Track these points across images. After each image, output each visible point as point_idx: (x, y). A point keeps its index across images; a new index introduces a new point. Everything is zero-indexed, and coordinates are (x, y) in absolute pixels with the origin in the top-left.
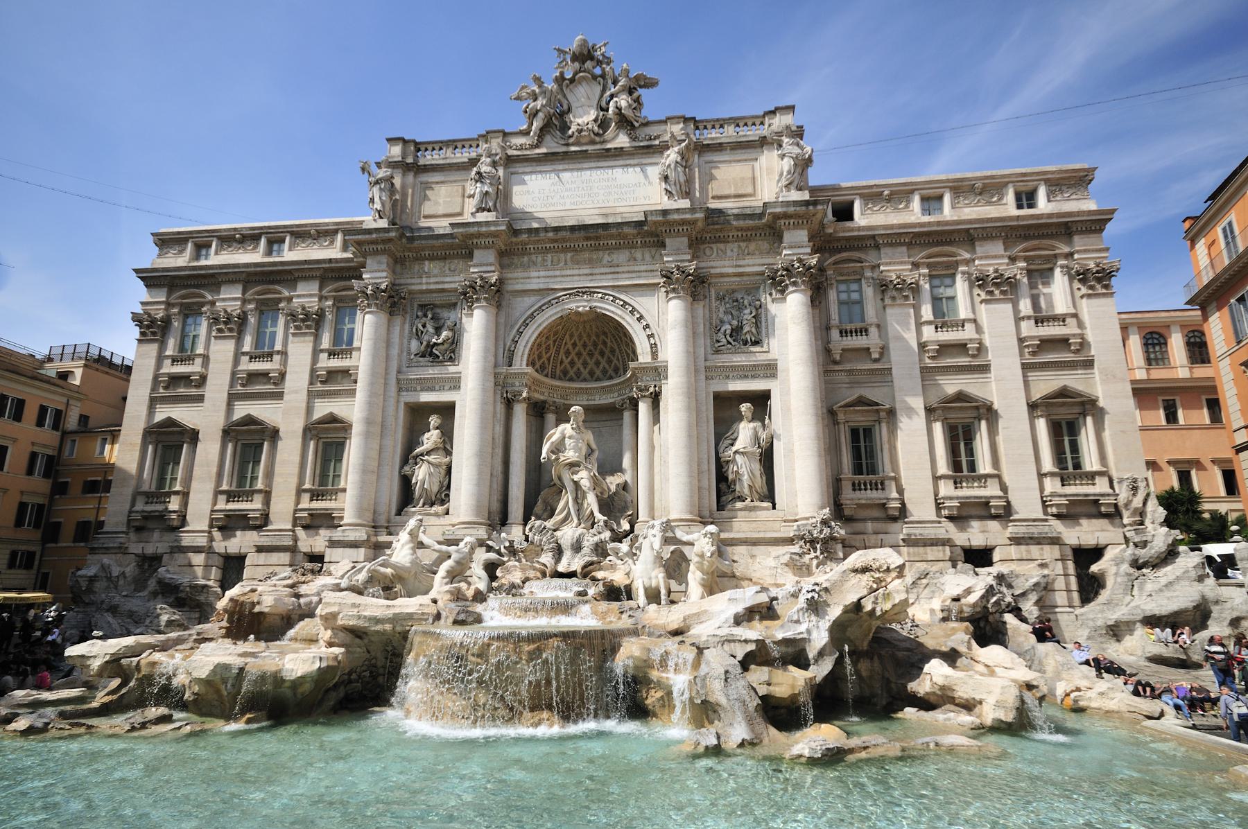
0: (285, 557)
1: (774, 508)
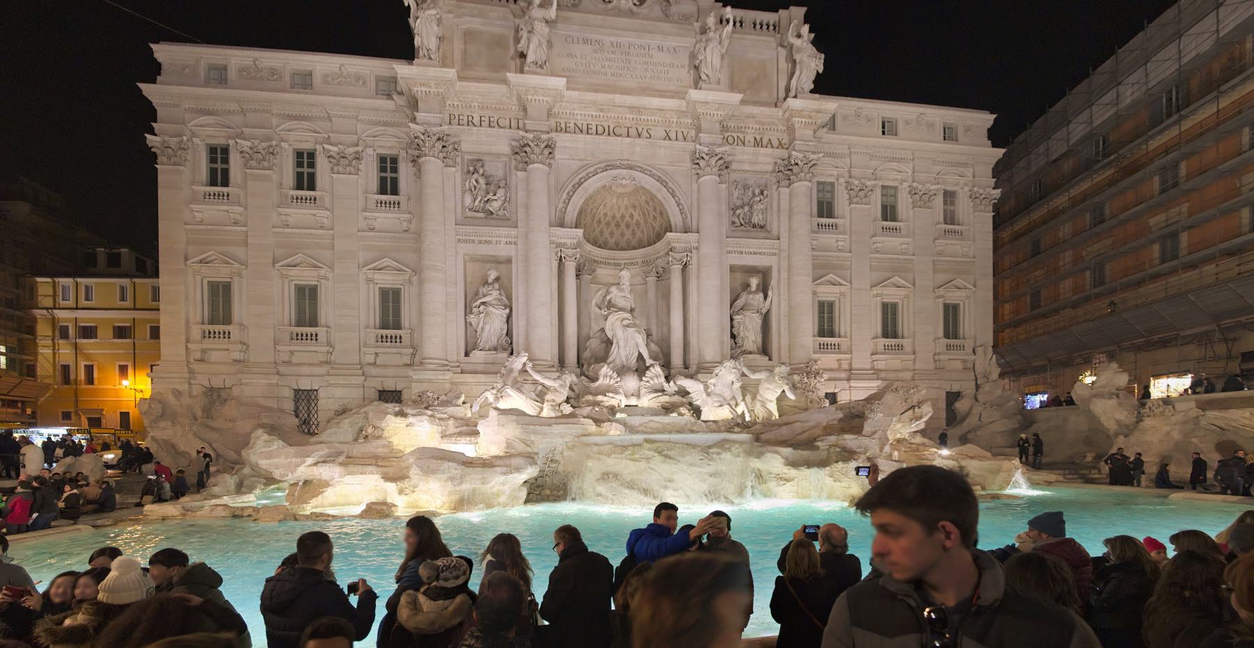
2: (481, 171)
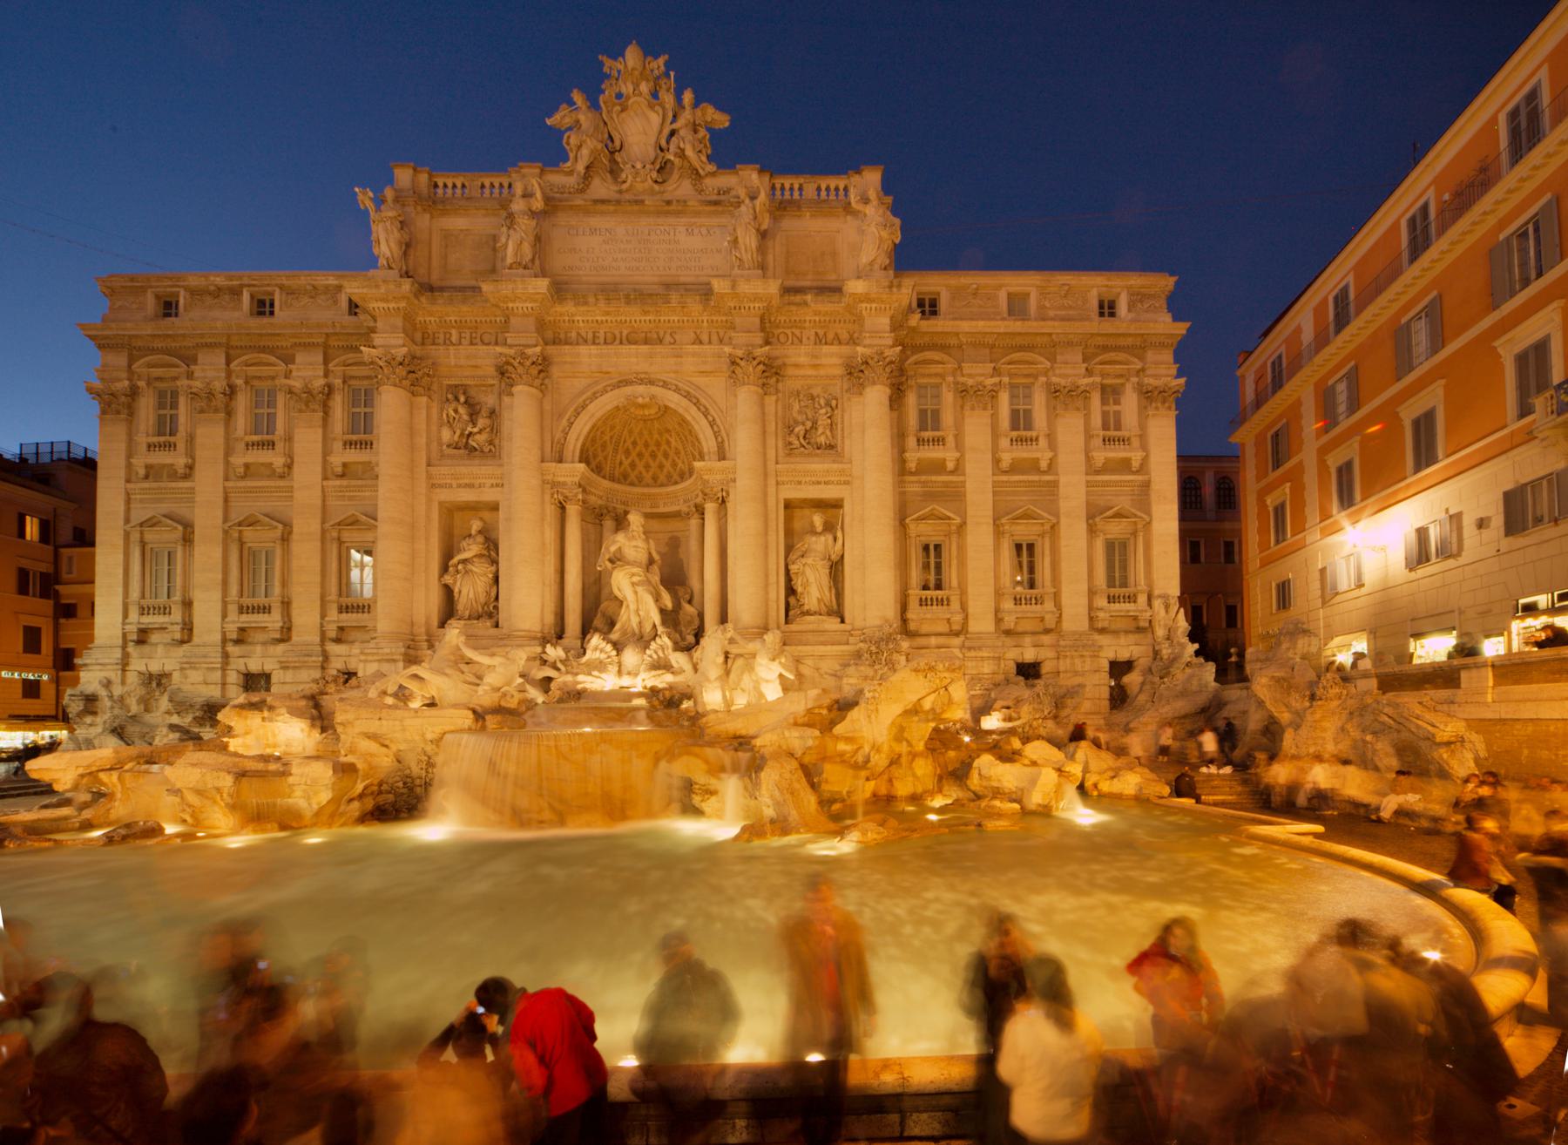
1: (843, 621)
2: (462, 399)
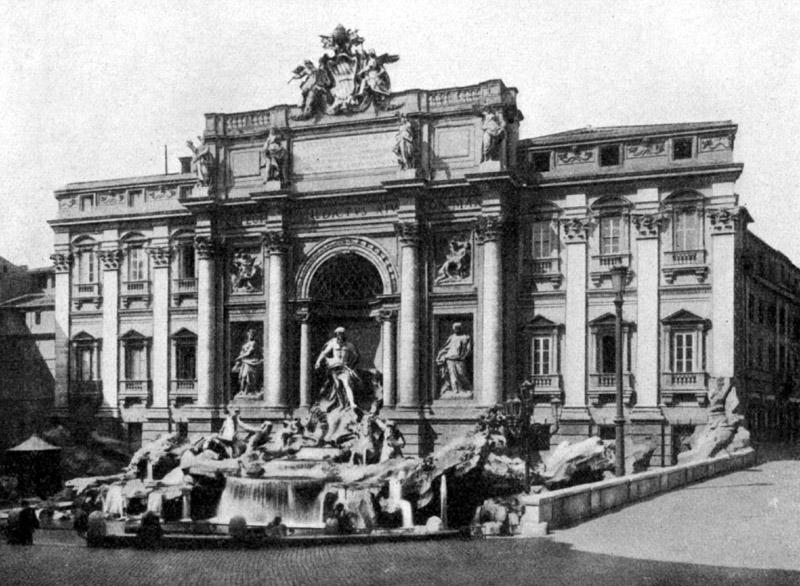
0: (165, 426)
